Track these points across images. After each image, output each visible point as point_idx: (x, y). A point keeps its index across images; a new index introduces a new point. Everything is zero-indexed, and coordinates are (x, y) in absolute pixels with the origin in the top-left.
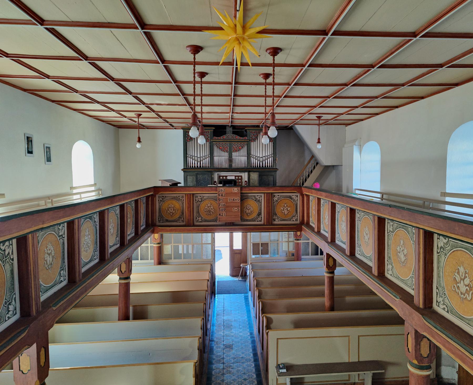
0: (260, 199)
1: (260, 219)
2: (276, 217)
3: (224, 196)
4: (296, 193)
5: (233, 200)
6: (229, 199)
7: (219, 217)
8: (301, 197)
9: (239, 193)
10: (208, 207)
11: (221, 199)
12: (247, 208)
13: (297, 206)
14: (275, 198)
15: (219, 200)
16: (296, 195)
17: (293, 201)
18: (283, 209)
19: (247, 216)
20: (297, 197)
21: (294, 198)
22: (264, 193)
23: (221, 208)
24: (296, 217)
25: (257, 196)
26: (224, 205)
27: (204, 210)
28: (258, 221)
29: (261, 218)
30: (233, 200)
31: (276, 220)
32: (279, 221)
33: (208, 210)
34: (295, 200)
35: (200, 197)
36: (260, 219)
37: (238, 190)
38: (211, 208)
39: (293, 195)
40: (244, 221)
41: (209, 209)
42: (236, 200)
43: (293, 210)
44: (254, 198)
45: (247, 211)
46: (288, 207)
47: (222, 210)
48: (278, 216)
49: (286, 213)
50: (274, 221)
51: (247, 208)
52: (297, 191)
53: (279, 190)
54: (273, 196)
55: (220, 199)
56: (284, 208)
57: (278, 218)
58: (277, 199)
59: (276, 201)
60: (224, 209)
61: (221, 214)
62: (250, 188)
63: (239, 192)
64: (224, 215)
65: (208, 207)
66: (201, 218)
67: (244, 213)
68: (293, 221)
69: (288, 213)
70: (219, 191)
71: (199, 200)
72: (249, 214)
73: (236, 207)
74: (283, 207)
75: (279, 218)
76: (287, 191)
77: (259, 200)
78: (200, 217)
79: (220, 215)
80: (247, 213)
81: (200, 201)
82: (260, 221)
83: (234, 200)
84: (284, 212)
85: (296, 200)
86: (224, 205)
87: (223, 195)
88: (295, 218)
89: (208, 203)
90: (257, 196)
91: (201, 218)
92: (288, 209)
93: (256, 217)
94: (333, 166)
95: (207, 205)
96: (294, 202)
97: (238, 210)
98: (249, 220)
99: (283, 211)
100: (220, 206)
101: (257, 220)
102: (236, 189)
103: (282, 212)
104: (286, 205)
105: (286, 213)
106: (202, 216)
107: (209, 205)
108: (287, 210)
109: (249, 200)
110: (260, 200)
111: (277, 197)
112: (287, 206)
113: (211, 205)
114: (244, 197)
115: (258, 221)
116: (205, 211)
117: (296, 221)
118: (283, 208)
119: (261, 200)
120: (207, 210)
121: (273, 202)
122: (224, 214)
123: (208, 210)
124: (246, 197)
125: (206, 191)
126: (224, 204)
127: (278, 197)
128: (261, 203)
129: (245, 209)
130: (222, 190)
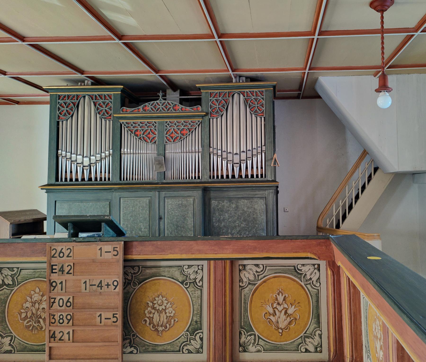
0: (199, 277)
1: (196, 344)
2: (249, 338)
3: (68, 273)
4: (311, 258)
5: (98, 286)
6: (85, 282)
7: (51, 345)
8: (329, 272)
9: (118, 261)
10: (33, 304)
11: (58, 282)
12: (154, 308)
13: (318, 301)
14: (247, 275)
15: (51, 284)
16: (314, 265)
17: (306, 285)
18: (271, 310)
19: (154, 334)
20: (319, 270)
21: (308, 274)
22: (209, 260)
23: (59, 314)
24: (317, 338)
25: (190, 266)
26: (69, 304)
27: (22, 313)
28: (192, 353)
29: (201, 339)
30: (98, 286)
31: (251, 348)
32: (259, 351)
33: (33, 313)
34: (311, 279)
35: (10, 273)
36: (196, 344)
37: (115, 253)
38: (41, 307)
39: (303, 265)
40: (146, 351)
41: (34, 311)
42: (108, 285)
43: (307, 315)
44: (177, 274)
45: (156, 317)
46: (289, 304)
47: (61, 321)
48: (257, 334)
49: (282, 325)
50: (245, 351)
51: (154, 308)
52: (315, 254)
53: (254, 249)
54: (241, 267)
55: (54, 284)
56: (275, 305)
57: (255, 340)
58: (252, 278)
59: (249, 284)
60: (69, 317)
61: (58, 336)
62: (159, 243)
63: (121, 256)
64: (66, 337)
65: (33, 304)
66: (9, 338)
67: (146, 323)
68: (307, 351)
69: (290, 323)
70: (53, 257)
71: (6, 282)
72: (160, 329)
73: (107, 308)
74: (272, 305)
75: (261, 343)
76: (285, 252)
77: (195, 279)
78: (7, 337)
79: (55, 337)
80: (155, 323)
81: (8, 285)
82: (198, 352)
83: (101, 287)
84: (278, 322)
85: (314, 279)
86: (69, 304)
87: (66, 269)
88: (312, 343)
89: (32, 292)
90: (190, 266)
91: (9, 338)
92: (290, 311)
93: (183, 339)
94: (414, 174)
95: (31, 298)
96: (309, 286)
97: (115, 319)
98: (160, 348)
99: (272, 317)
100: (56, 305)
101: (189, 347)
102: (107, 247)
103: (270, 321)
104: (281, 298)
105: (282, 325)
106: (14, 334)
107: (36, 297)
108: (286, 313)
109: (162, 281)
110: (197, 281)
111: (251, 269)
112: (284, 299)
113: (43, 296)
114: (148, 271)
115: (190, 352)
116: (23, 315)
117: (316, 351)
118: (273, 308)
119: (202, 280)
120: (29, 315)
121: (240, 286)
122: (69, 333)
123: (33, 313)
124: (154, 270)
125: (16, 256)
126: (68, 301)
127: (255, 269)
128: (201, 290)
129: (149, 309)
130: (61, 252)
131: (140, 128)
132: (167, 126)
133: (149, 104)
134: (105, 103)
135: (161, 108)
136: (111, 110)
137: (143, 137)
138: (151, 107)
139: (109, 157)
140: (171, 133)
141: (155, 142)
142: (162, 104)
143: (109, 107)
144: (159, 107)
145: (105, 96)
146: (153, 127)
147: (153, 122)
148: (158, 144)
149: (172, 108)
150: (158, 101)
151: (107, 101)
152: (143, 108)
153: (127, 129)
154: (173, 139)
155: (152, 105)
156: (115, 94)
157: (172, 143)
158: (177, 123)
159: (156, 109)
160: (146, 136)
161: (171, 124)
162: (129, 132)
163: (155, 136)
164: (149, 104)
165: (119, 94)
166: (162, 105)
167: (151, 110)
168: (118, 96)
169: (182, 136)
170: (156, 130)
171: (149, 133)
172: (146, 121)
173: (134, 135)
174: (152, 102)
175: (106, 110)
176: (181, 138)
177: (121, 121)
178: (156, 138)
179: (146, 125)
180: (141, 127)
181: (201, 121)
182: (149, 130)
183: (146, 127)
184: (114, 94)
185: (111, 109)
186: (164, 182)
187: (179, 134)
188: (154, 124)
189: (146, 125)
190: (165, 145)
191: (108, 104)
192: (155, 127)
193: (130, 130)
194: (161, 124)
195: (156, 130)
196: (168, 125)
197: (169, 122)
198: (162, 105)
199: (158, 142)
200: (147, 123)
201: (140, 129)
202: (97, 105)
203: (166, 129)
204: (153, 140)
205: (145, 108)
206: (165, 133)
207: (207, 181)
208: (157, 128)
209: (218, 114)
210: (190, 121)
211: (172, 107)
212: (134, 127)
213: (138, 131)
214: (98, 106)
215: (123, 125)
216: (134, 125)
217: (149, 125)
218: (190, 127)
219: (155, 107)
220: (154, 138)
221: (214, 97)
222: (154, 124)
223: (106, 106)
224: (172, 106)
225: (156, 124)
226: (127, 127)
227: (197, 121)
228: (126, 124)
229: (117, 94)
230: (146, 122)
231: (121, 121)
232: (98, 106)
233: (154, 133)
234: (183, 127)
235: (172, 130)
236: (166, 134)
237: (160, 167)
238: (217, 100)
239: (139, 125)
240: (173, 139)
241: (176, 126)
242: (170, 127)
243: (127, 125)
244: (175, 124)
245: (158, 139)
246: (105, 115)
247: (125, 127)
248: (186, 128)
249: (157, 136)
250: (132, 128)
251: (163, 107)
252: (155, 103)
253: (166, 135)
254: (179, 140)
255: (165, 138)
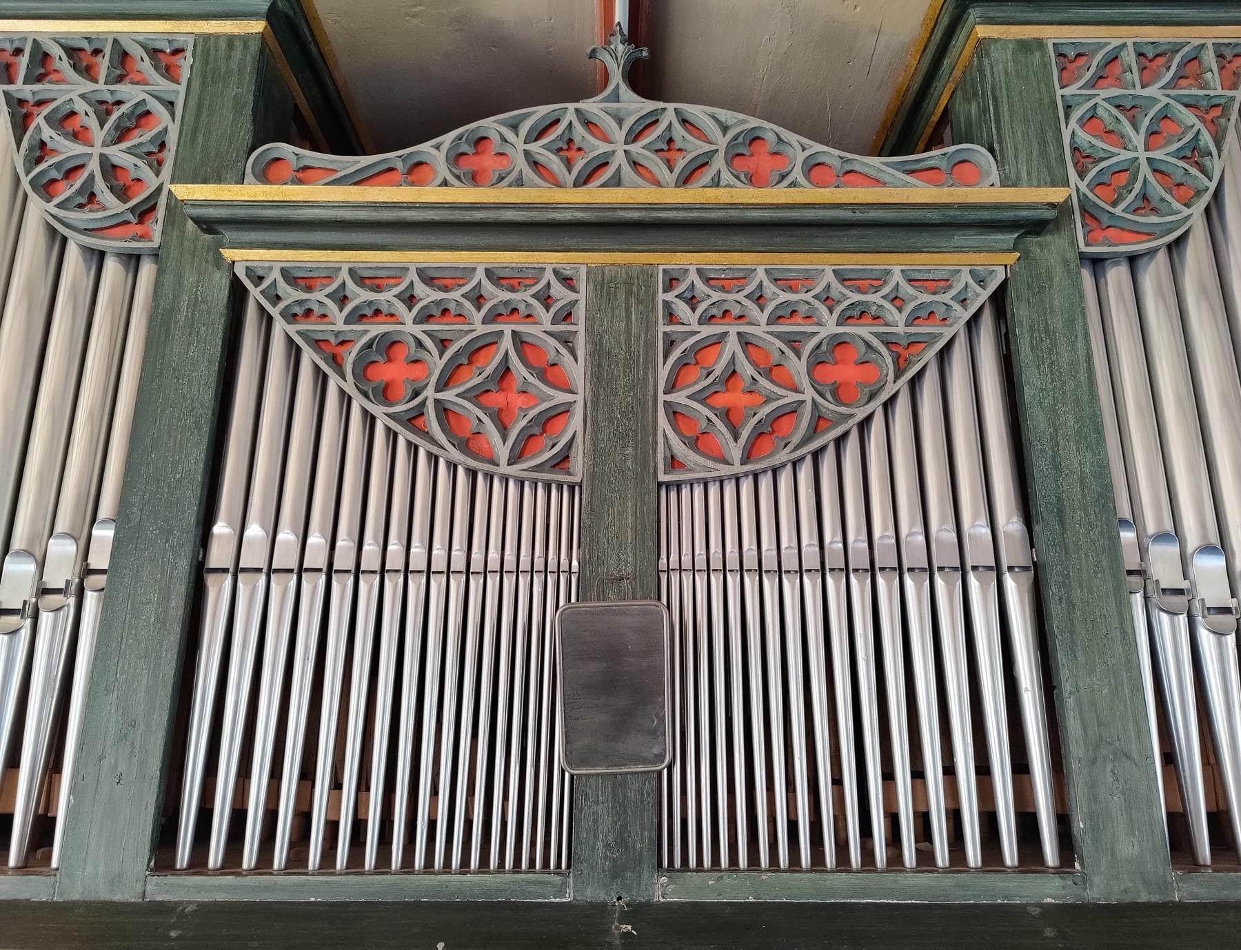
131: (416, 322)
132: (682, 309)
133: (515, 127)
134: (109, 113)
135: (620, 159)
136: (157, 167)
137: (444, 411)
138: (535, 147)
139: (72, 601)
140: (717, 372)
141: (561, 462)
142: (627, 126)
143: (141, 137)
144: (603, 148)
145: (122, 56)
146: (545, 317)
147: (549, 275)
148: (592, 477)
149: (719, 163)
150: (591, 106)
151: (131, 93)
152: (456, 158)
153: (292, 330)
154: (745, 433)
155: (539, 133)
156: (217, 36)
157: (738, 469)
158: (770, 288)
159: (579, 165)
160: (477, 395)
161: (716, 296)
162: (309, 356)
163: (562, 397)
164: (515, 127)
165: (245, 39)
166: (634, 136)
167: (528, 173)
168: (237, 54)
169: (828, 406)
170: (566, 341)
171: (505, 371)
172: (481, 260)
173: (350, 388)
174: (542, 111)
175: (110, 169)
176: (819, 422)
177: (241, 257)
178: (576, 423)
179: (478, 299)
180: (425, 317)
181: (1000, 275)
182: (507, 343)
183: (478, 317)
184: (207, 37)
185: (160, 163)
186: (658, 898)
187: (796, 390)
188: (558, 290)
189: (478, 299)
190: (660, 484)
191: (142, 116)
192: (566, 316)
193: (317, 344)
194: (622, 296)
195: (566, 341)
196: (692, 301)
197: (693, 277)
198: (634, 136)
199: (595, 453)
200: (486, 283)
201: (417, 330)
202: (39, 120)
203: (670, 344)
204: (545, 440)
205: (476, 159)
206: (663, 372)
207: (1144, 898)
208: (581, 328)
209: (1155, 219)
210: (897, 277)
211: (721, 154)
212: (357, 317)
213: (397, 350)
214: (47, 133)
215: (255, 292)
216: (364, 295)
217: (506, 296)
218: (901, 329)
219: (567, 147)
220: (550, 419)
221: (1094, 83)
222: (558, 290)
223: (121, 134)
224: (722, 142)
225: (572, 296)
226: (290, 317)
227: (965, 277)
228: (283, 288)
229: (231, 39)
230: (480, 274)
231: (241, 257)
232: (47, 133)
233: (549, 373)
234: (830, 326)
235: (732, 345)
236: (671, 387)
237: (622, 725)
238: (1131, 109)
239: (409, 299)
240: (745, 433)
241: (763, 318)
242: (708, 319)
243: (291, 294)
244: (759, 299)
245: (593, 423)
246: (104, 208)
247: (274, 312)
248: (864, 331)
249: (579, 399)
250: (340, 326)
251: (635, 148)
252: (570, 116)
253: (674, 397)
254: (797, 448)
255: (663, 421)
